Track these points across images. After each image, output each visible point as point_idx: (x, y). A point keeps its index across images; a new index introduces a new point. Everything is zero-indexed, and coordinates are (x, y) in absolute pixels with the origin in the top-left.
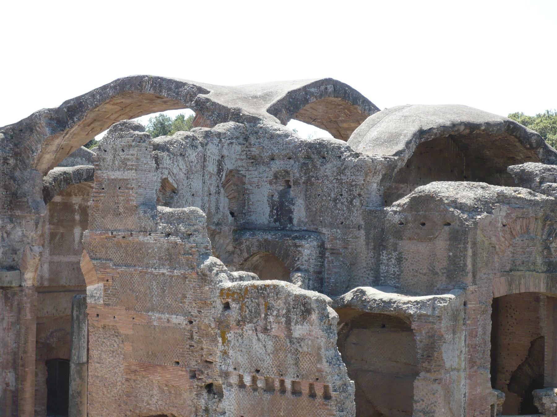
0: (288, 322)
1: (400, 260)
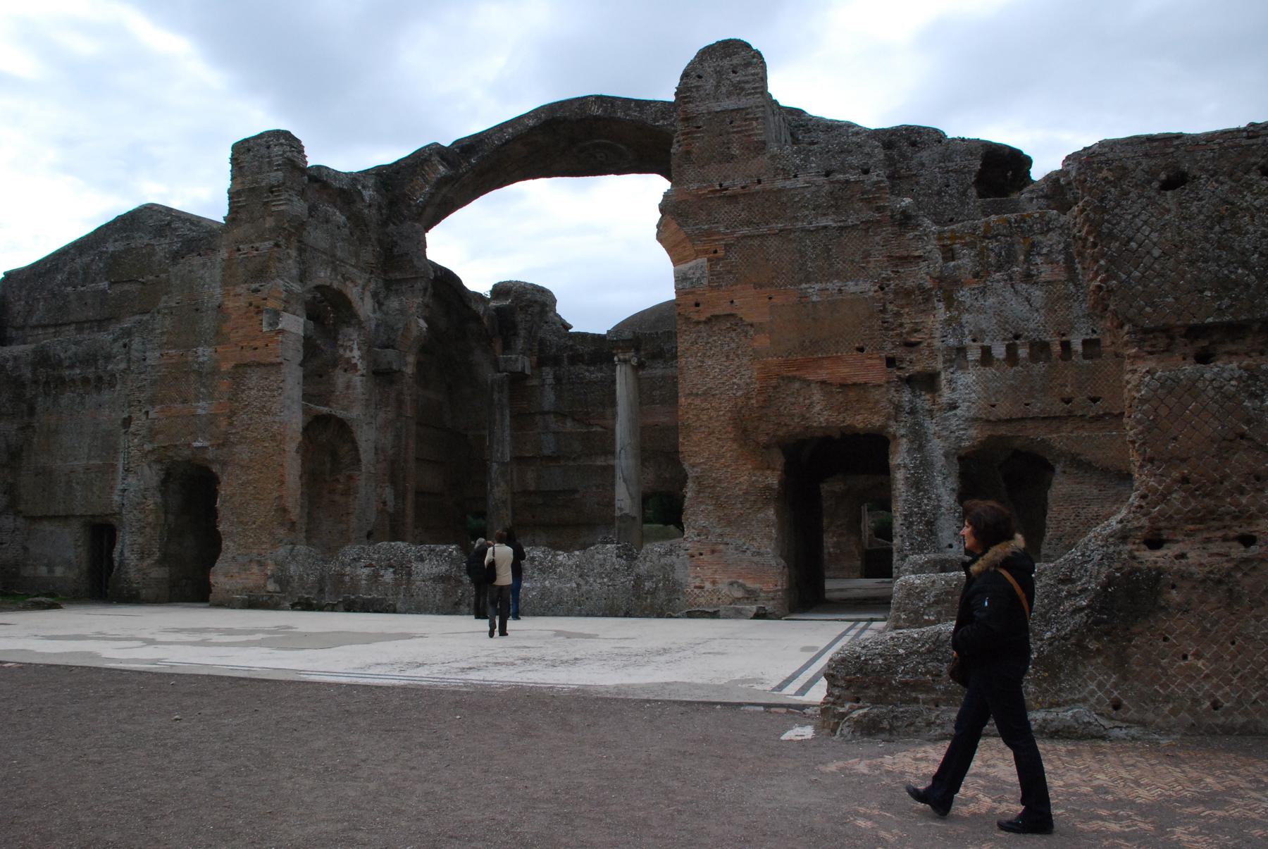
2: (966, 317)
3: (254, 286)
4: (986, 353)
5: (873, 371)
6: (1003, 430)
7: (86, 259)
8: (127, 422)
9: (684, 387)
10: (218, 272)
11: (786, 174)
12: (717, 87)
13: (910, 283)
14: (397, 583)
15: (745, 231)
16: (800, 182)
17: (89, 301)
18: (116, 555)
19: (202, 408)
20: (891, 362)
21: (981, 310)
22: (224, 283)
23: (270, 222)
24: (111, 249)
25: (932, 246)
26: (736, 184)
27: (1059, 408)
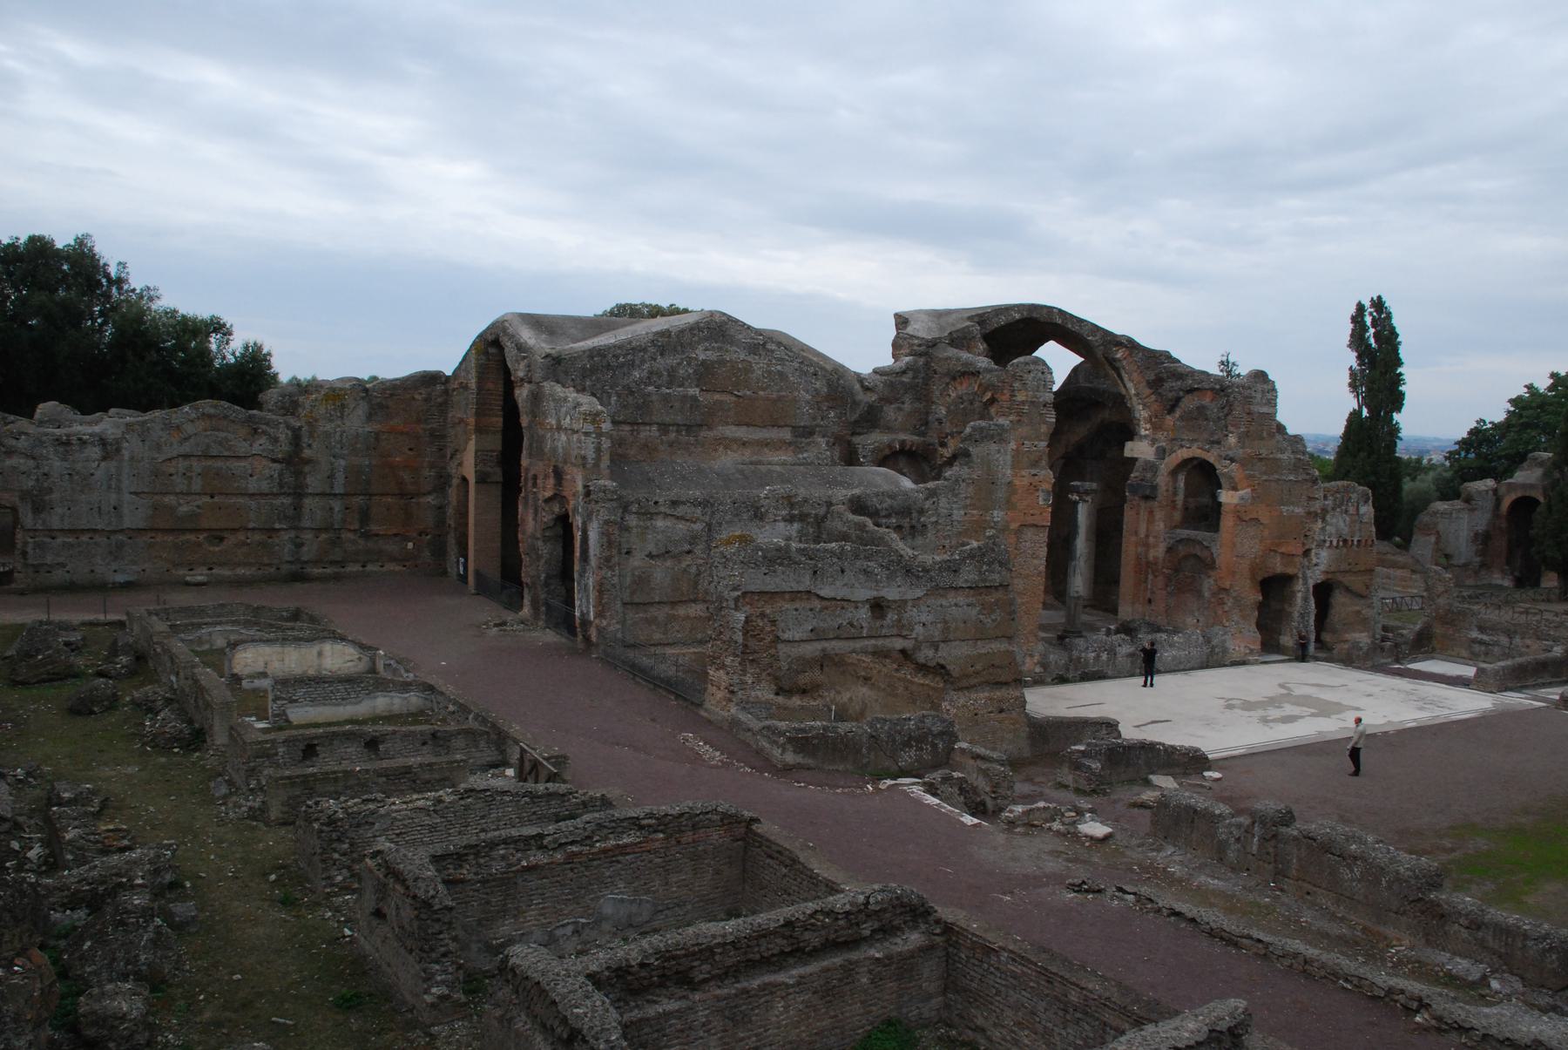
7: (671, 361)
16: (1284, 457)
17: (677, 405)
22: (1013, 467)
24: (702, 357)
26: (1264, 452)
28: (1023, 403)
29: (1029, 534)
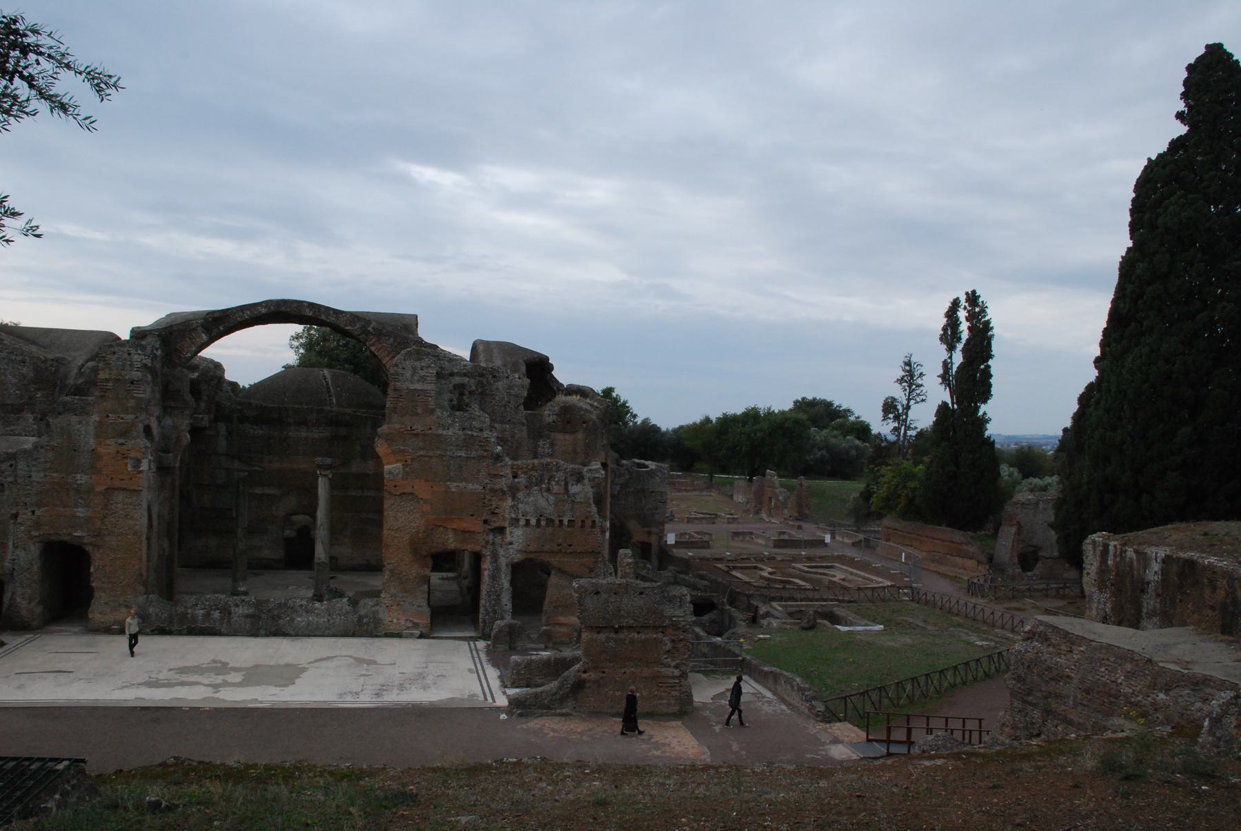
0: (566, 484)
1: (552, 445)
2: (520, 506)
3: (121, 441)
4: (528, 521)
5: (476, 526)
6: (532, 556)
8: (15, 516)
9: (386, 526)
10: (92, 429)
11: (444, 427)
12: (412, 376)
13: (497, 487)
14: (222, 618)
15: (422, 453)
18: (6, 600)
19: (81, 512)
20: (485, 522)
21: (527, 503)
22: (97, 436)
23: (132, 403)
25: (508, 472)
26: (418, 428)
27: (556, 548)
28: (107, 380)
29: (120, 497)
